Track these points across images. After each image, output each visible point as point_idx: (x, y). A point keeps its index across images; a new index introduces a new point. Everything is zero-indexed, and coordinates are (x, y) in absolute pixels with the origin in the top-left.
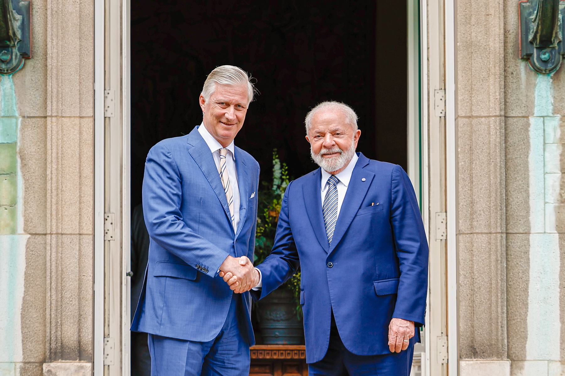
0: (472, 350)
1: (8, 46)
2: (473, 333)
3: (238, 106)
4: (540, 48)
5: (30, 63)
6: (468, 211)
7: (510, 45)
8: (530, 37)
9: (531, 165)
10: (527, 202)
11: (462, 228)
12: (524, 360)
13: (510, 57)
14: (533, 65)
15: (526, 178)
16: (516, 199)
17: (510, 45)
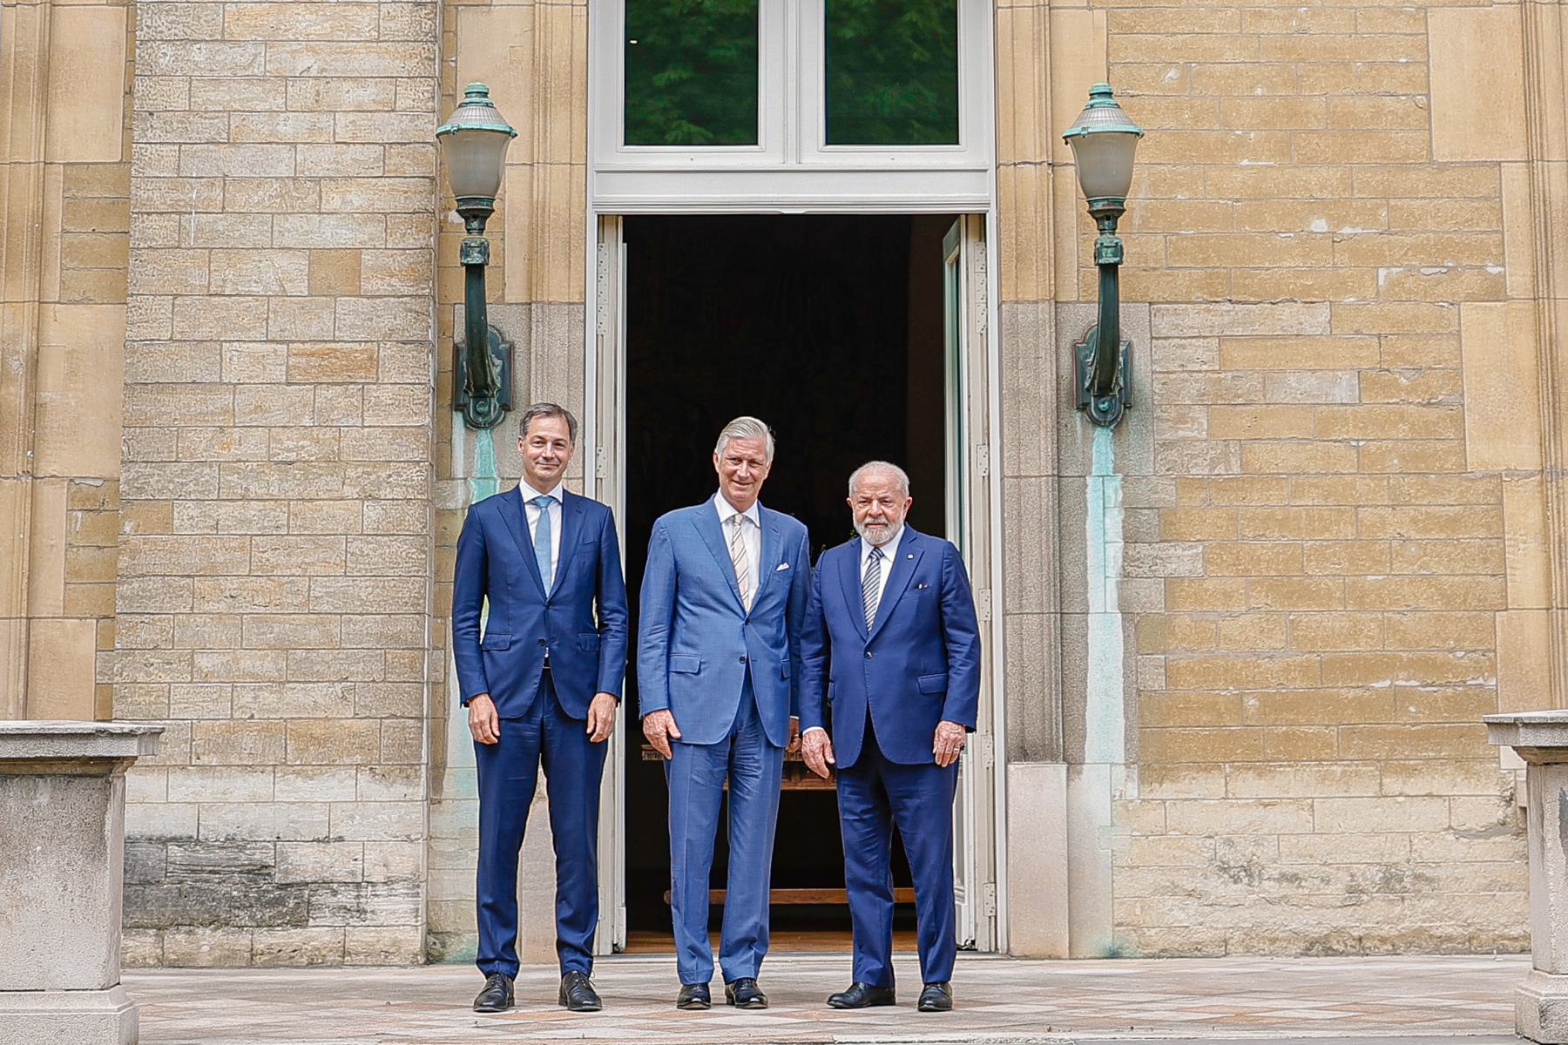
0: (1021, 752)
1: (485, 397)
5: (511, 416)
6: (1015, 588)
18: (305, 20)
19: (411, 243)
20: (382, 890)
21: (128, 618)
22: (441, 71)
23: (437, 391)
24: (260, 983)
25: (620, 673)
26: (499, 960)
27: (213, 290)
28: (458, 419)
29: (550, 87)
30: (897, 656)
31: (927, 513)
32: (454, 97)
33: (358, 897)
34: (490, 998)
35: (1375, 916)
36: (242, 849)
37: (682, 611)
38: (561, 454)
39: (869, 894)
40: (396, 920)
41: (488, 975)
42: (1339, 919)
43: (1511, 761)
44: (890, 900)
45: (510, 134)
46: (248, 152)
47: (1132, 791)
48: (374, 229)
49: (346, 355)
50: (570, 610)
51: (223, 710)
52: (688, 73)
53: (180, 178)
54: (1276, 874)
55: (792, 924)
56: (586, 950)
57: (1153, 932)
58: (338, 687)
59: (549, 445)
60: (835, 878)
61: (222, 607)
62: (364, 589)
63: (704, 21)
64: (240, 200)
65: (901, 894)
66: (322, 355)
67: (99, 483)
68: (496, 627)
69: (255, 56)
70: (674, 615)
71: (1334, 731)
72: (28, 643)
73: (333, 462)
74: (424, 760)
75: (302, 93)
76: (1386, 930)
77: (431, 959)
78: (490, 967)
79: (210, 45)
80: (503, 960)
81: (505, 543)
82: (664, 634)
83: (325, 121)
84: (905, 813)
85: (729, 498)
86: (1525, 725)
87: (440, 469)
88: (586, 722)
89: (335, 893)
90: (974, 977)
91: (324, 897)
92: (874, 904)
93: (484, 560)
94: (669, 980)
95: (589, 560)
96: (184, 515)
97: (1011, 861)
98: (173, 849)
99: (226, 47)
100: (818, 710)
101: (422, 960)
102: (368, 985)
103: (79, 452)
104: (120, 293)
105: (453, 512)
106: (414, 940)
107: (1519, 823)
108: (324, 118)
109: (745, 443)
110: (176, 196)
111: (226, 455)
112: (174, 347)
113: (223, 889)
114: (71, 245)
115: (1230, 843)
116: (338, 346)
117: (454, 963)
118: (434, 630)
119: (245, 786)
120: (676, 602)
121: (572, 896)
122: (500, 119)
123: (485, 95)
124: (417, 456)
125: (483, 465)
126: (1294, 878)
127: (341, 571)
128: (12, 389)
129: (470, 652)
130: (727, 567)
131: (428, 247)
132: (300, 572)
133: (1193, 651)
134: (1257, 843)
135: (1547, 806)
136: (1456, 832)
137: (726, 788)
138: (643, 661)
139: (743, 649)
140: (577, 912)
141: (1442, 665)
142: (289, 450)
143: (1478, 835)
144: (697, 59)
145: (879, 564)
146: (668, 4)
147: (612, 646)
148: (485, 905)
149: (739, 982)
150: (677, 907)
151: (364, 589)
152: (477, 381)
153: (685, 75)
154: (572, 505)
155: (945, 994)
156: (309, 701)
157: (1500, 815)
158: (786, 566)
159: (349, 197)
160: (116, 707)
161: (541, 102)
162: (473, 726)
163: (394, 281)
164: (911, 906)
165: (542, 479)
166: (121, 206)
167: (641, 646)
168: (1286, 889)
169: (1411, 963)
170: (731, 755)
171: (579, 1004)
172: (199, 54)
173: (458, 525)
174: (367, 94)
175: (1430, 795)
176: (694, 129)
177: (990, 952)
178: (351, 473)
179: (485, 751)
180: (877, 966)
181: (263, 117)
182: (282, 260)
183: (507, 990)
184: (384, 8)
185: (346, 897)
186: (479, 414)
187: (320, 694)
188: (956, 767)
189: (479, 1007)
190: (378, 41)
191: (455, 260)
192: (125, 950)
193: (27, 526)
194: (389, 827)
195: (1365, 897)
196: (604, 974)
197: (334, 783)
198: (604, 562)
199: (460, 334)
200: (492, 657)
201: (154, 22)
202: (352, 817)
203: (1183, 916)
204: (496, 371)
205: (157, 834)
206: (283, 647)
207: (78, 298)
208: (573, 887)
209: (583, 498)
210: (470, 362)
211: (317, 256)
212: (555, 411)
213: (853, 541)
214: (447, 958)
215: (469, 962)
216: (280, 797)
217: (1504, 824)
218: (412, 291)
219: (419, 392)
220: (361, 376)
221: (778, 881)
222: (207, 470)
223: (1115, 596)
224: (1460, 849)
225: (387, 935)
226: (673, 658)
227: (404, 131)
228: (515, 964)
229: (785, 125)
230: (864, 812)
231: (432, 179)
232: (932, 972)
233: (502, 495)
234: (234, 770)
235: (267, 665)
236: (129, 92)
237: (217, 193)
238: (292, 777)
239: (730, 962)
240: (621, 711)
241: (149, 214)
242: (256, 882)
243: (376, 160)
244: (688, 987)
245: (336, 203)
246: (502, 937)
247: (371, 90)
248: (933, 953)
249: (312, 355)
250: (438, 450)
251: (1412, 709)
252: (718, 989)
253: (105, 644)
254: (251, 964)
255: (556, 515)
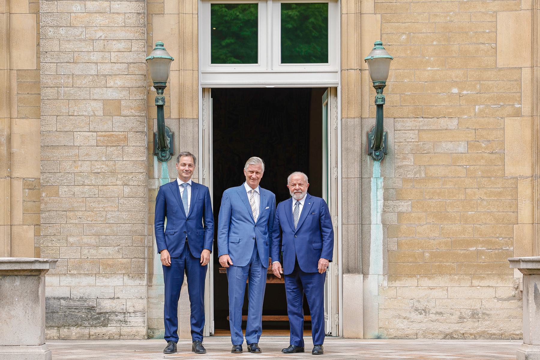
0: (348, 270)
2: (348, 264)
3: (257, 173)
4: (375, 151)
6: (346, 216)
7: (363, 149)
8: (372, 146)
9: (372, 197)
10: (370, 212)
11: (344, 222)
12: (368, 274)
13: (363, 154)
14: (373, 157)
15: (370, 202)
16: (365, 210)
17: (363, 149)
18: (99, 20)
19: (138, 98)
20: (132, 315)
21: (45, 225)
22: (147, 38)
23: (148, 149)
24: (92, 345)
25: (211, 243)
26: (172, 337)
27: (70, 114)
28: (155, 158)
29: (186, 43)
30: (305, 236)
31: (315, 188)
32: (152, 47)
33: (124, 317)
34: (169, 349)
35: (469, 326)
36: (85, 301)
37: (233, 222)
38: (191, 169)
39: (296, 316)
40: (138, 325)
41: (168, 342)
42: (457, 327)
43: (518, 275)
44: (303, 318)
45: (171, 60)
46: (80, 66)
47: (385, 284)
48: (125, 93)
49: (117, 136)
50: (194, 222)
51: (78, 255)
52: (233, 38)
53: (57, 75)
54: (434, 312)
55: (269, 327)
56: (201, 334)
57: (392, 330)
58: (117, 248)
59: (187, 166)
60: (284, 312)
61: (77, 221)
62: (125, 215)
63: (239, 22)
64: (78, 83)
65: (307, 318)
66: (109, 136)
67: (33, 180)
68: (170, 227)
69: (82, 32)
70: (230, 223)
71: (455, 265)
72: (11, 233)
73: (113, 173)
74: (146, 272)
75: (99, 45)
76: (472, 331)
77: (149, 337)
78: (168, 339)
79: (66, 28)
80: (173, 337)
81: (172, 199)
82: (227, 229)
83: (107, 54)
84: (308, 289)
85: (249, 184)
86: (523, 261)
87: (150, 175)
88: (200, 259)
89: (117, 316)
90: (331, 344)
91: (113, 317)
92: (297, 319)
93: (165, 205)
94: (228, 344)
95: (201, 205)
96: (63, 190)
97: (344, 307)
98: (62, 301)
99: (71, 29)
100: (277, 256)
101: (146, 337)
102: (128, 345)
103: (26, 169)
104: (38, 116)
105: (154, 190)
106: (143, 331)
107: (519, 296)
108: (107, 54)
109: (255, 166)
110: (56, 81)
111: (76, 170)
112: (57, 133)
113: (79, 314)
114: (20, 98)
115: (419, 301)
116: (114, 133)
117: (157, 339)
118: (149, 229)
119: (86, 281)
120: (231, 219)
121: (196, 316)
122: (168, 54)
123: (163, 46)
124: (142, 171)
125: (164, 173)
126: (441, 313)
127: (116, 209)
128: (2, 148)
129: (161, 235)
130: (249, 207)
131: (144, 99)
132: (103, 210)
133: (407, 237)
134: (428, 302)
135: (530, 289)
136: (498, 299)
137: (247, 282)
138: (220, 238)
139: (254, 235)
140: (198, 321)
141: (494, 242)
142: (98, 169)
143: (505, 300)
144: (237, 36)
145: (299, 206)
146: (226, 16)
147: (209, 234)
148: (167, 319)
149: (252, 345)
150: (231, 320)
151: (125, 215)
152: (162, 145)
153: (233, 41)
154: (195, 186)
155: (321, 349)
156: (107, 252)
157: (513, 293)
158: (268, 208)
159: (116, 82)
160: (42, 254)
161: (182, 49)
162: (162, 260)
163: (132, 111)
164: (310, 322)
165: (185, 178)
166: (37, 84)
167: (219, 233)
168: (438, 317)
169: (480, 342)
170: (250, 270)
171: (199, 351)
172: (62, 31)
173: (156, 193)
174: (121, 46)
175: (489, 286)
176: (236, 60)
177: (336, 336)
178: (119, 176)
179: (166, 268)
180: (298, 339)
181: (86, 54)
182: (93, 104)
183: (174, 346)
184: (127, 15)
185: (121, 317)
186: (163, 156)
187: (110, 250)
188: (325, 274)
189: (165, 352)
190: (125, 27)
191: (153, 104)
192: (47, 334)
193: (9, 194)
194: (134, 294)
195: (465, 320)
196: (206, 342)
197: (116, 280)
198: (206, 205)
199: (155, 129)
200: (168, 237)
201: (45, 20)
202: (122, 291)
203: (402, 325)
204: (168, 142)
205: (56, 296)
206: (97, 235)
207: (23, 117)
208: (196, 313)
209: (198, 184)
210: (160, 139)
211: (106, 102)
212: (189, 154)
213: (289, 199)
214: (155, 337)
215: (162, 338)
216: (98, 284)
217: (514, 296)
218: (139, 114)
219: (142, 149)
220: (122, 144)
221: (265, 313)
222: (70, 175)
223: (380, 218)
224: (499, 304)
225: (134, 330)
226: (230, 238)
227: (134, 59)
228: (177, 338)
229: (267, 57)
230: (294, 289)
231: (145, 75)
232: (317, 341)
233: (171, 183)
234: (82, 276)
235: (93, 240)
236: (38, 45)
237: (70, 80)
238: (102, 278)
239: (249, 338)
240: (212, 256)
241: (47, 87)
242: (90, 312)
243: (125, 69)
244: (235, 346)
245: (112, 84)
246: (173, 329)
247: (123, 44)
248: (317, 335)
249: (105, 136)
250: (149, 169)
251: (483, 257)
252: (245, 346)
253: (37, 234)
254: (89, 339)
255: (189, 190)
